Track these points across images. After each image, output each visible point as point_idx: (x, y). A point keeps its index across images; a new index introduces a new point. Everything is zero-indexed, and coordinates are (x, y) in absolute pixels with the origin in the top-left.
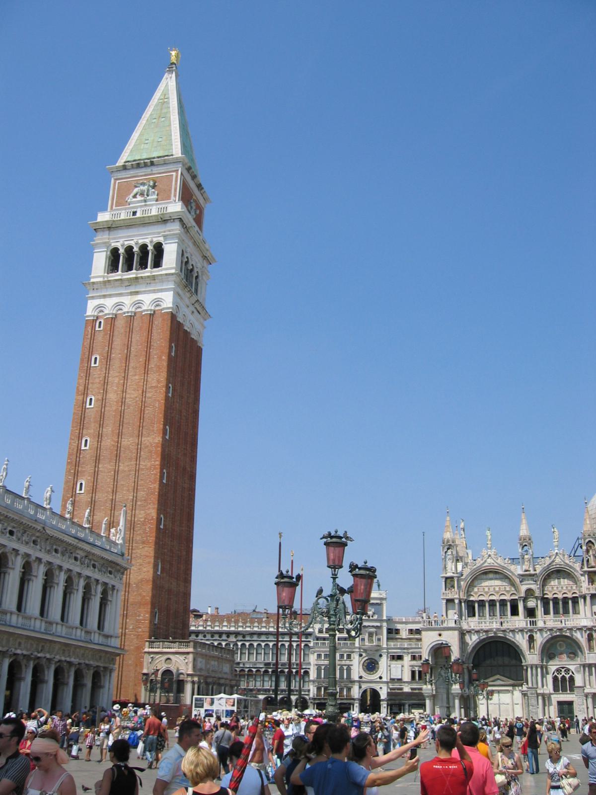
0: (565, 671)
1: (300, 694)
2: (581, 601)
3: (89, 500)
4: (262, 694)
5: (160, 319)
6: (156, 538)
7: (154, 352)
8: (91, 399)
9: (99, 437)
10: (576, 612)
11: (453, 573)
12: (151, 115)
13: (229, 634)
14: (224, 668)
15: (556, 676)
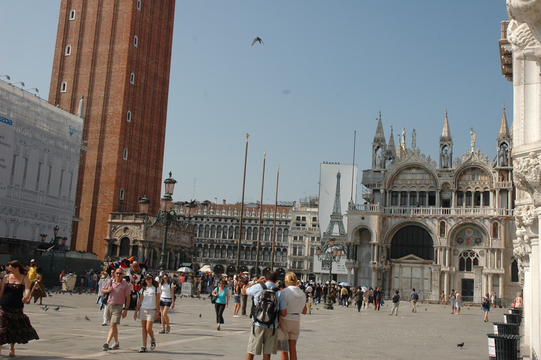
0: (471, 253)
2: (491, 194)
3: (70, 98)
4: (250, 265)
6: (121, 129)
9: (80, 45)
10: (487, 203)
11: (381, 168)
13: (226, 219)
15: (462, 258)
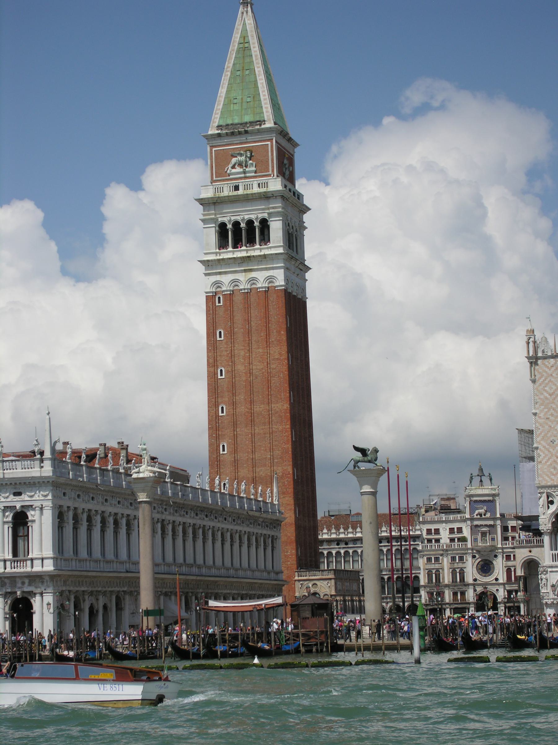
1: (412, 601)
3: (233, 459)
5: (275, 296)
7: (273, 326)
8: (221, 370)
12: (234, 64)
14: (354, 587)
